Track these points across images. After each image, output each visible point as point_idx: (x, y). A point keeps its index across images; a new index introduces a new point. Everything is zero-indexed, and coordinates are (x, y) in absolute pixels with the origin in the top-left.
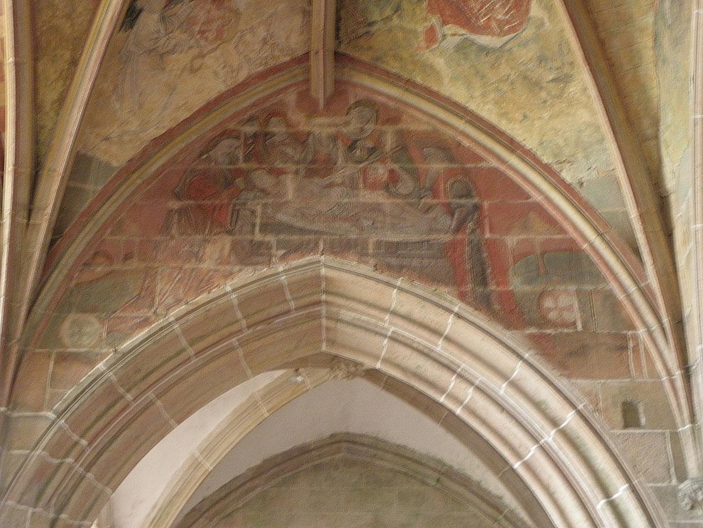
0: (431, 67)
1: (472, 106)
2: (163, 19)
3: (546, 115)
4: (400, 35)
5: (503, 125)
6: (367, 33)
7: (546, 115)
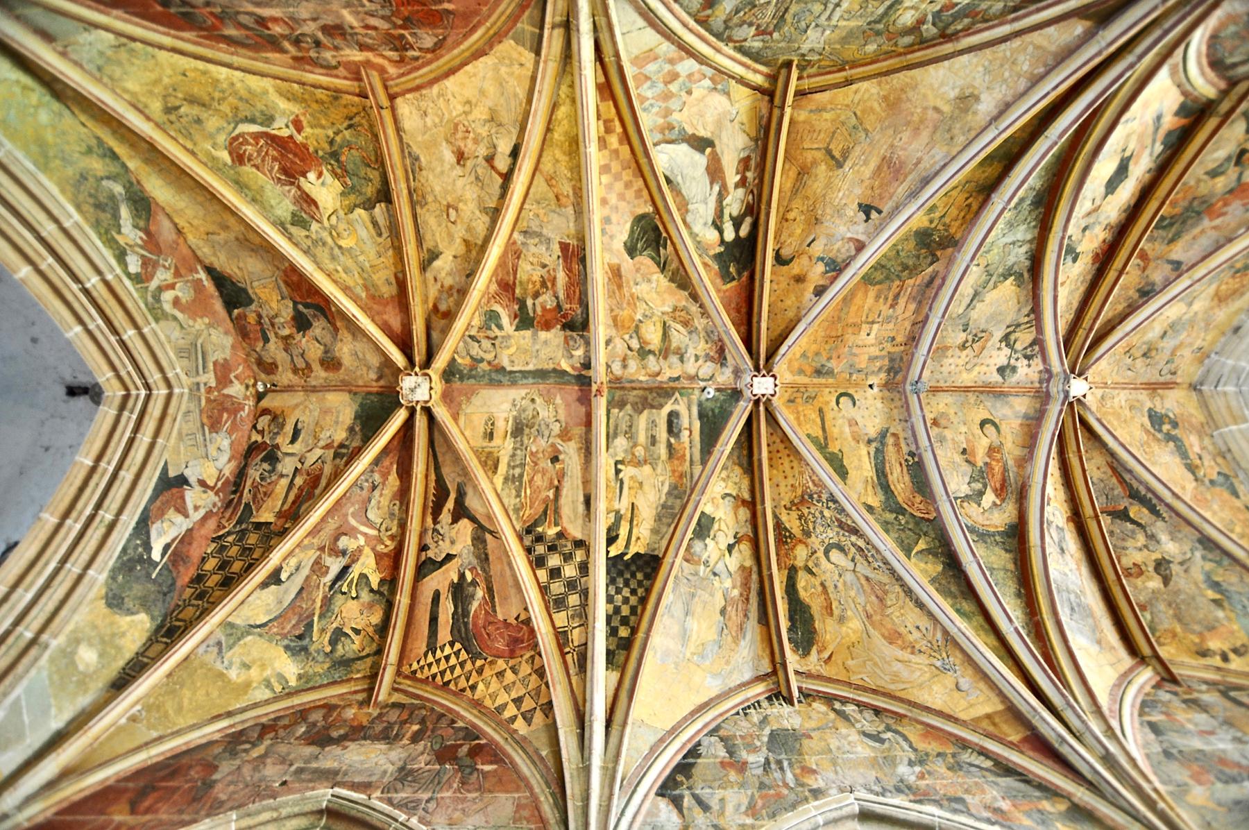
0: (289, 99)
1: (238, 74)
2: (495, 147)
3: (166, 80)
4: (323, 122)
5: (200, 65)
6: (351, 119)
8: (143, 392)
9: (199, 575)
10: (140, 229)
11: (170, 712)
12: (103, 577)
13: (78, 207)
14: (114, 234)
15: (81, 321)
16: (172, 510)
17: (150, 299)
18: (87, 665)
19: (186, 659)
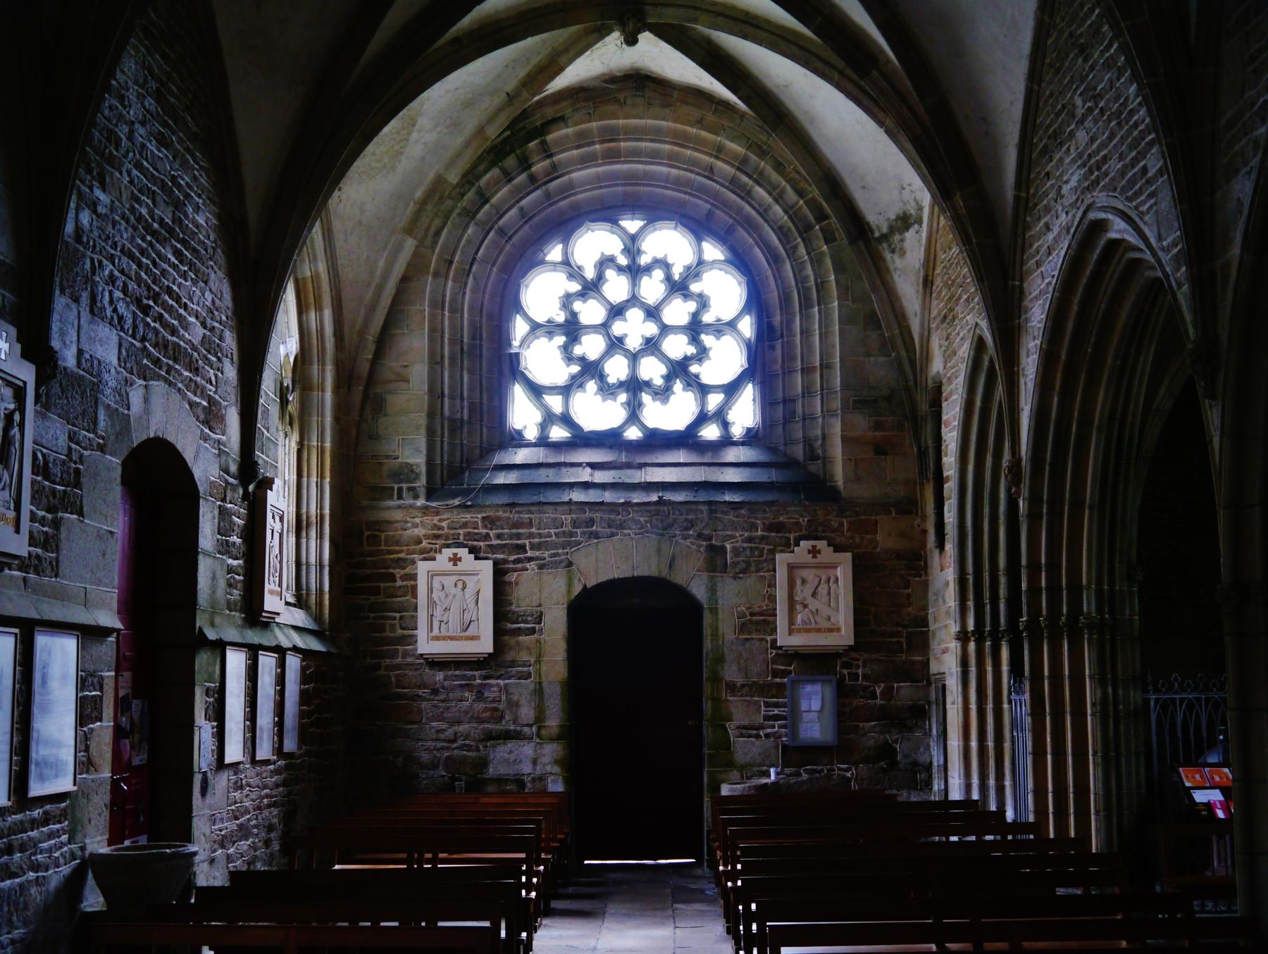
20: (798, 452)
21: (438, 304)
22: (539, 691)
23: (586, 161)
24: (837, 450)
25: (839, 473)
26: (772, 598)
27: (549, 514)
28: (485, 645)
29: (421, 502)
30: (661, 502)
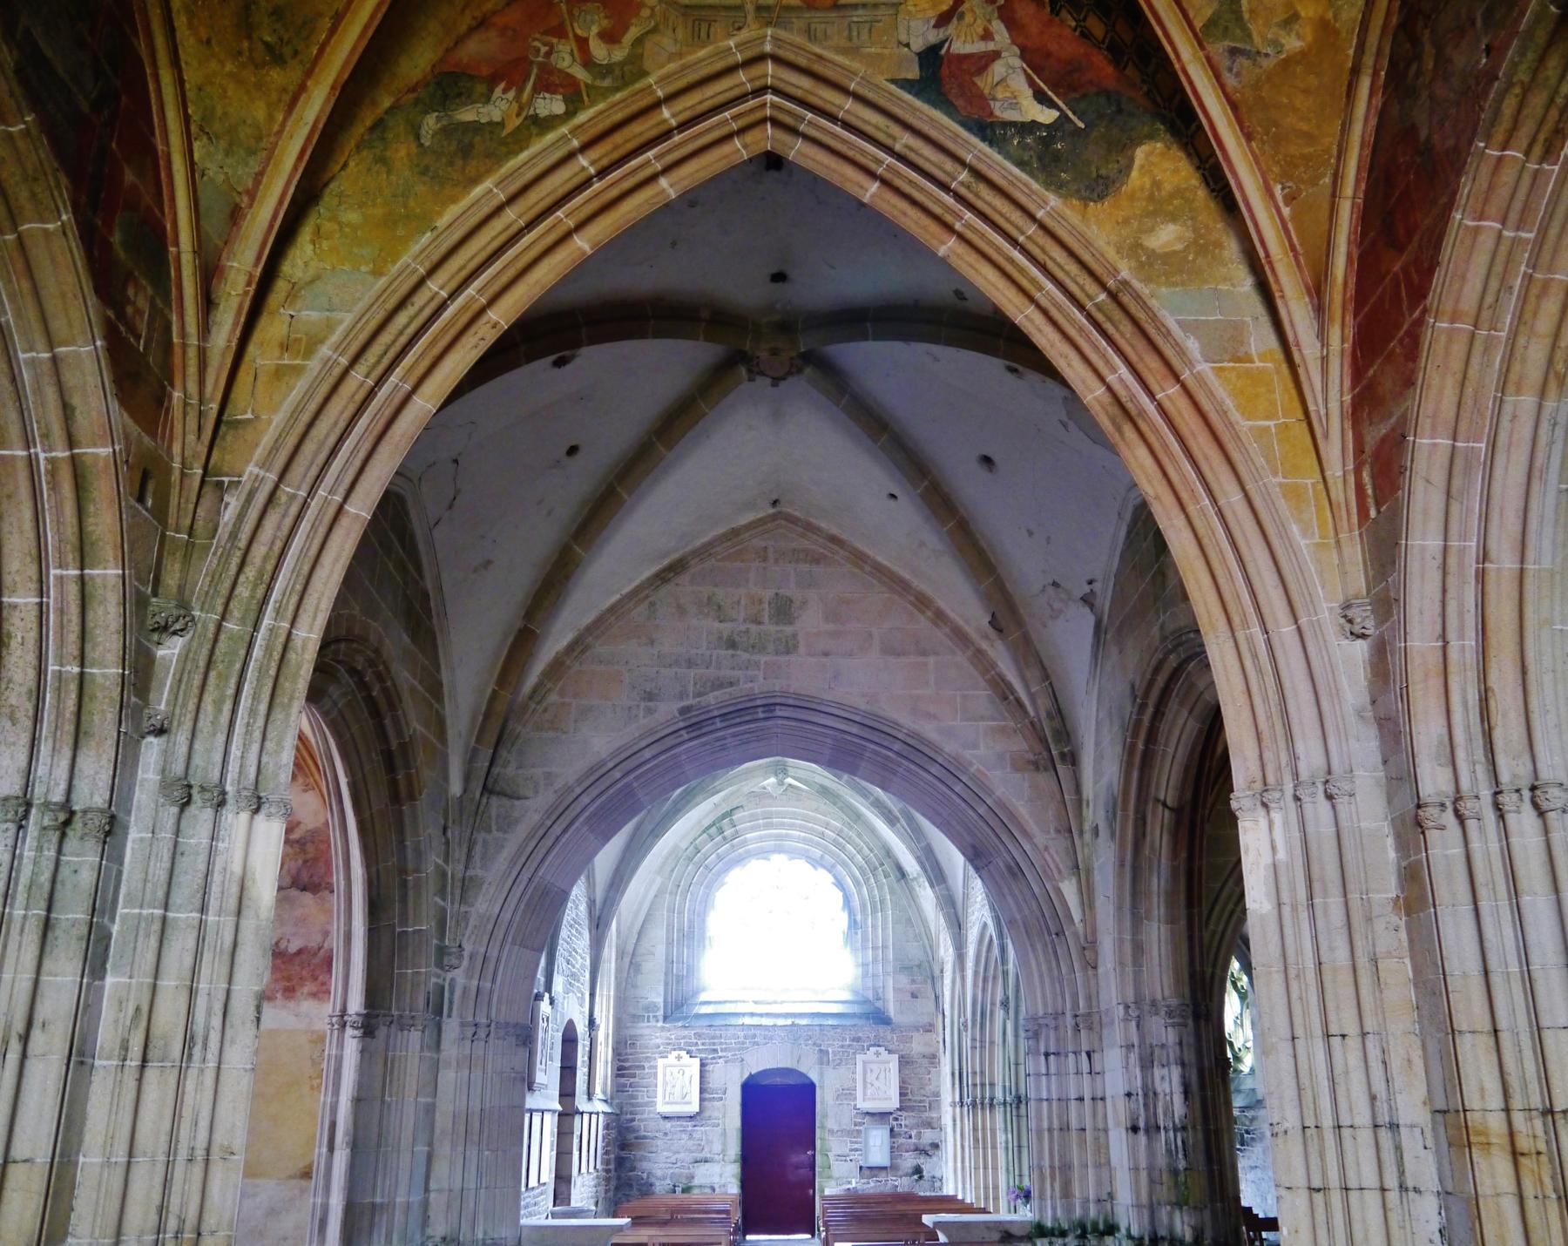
7: (229, 67)
8: (769, 97)
9: (1108, 49)
10: (491, 91)
11: (1306, 151)
12: (1053, 200)
13: (475, 181)
14: (504, 133)
15: (653, 178)
16: (979, 81)
17: (607, 83)
18: (1180, 239)
19: (1234, 106)
20: (870, 995)
21: (671, 910)
22: (724, 1134)
23: (753, 829)
24: (890, 995)
25: (891, 1010)
26: (854, 1080)
27: (731, 1031)
28: (695, 1108)
29: (660, 1024)
30: (793, 1024)
